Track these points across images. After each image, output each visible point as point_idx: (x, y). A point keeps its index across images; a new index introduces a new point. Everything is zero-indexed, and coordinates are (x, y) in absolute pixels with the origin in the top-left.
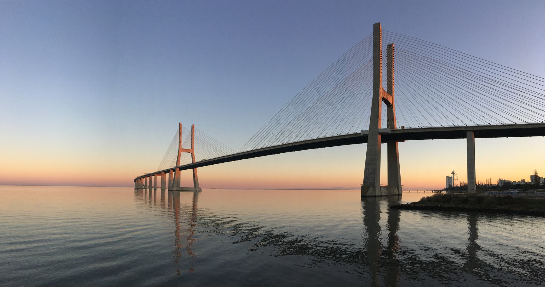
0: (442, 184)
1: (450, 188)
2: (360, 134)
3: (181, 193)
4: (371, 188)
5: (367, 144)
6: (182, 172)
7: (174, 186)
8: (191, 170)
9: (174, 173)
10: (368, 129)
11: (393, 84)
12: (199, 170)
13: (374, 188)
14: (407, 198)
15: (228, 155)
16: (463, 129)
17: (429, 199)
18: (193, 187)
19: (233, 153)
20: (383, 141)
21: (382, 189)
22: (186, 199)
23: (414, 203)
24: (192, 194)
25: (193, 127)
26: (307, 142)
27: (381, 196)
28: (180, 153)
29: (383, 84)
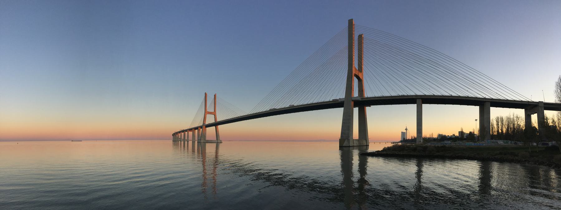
1: (404, 140)
5: (343, 108)
6: (207, 128)
7: (202, 139)
8: (214, 127)
9: (201, 129)
10: (344, 97)
11: (363, 64)
12: (220, 127)
13: (348, 140)
15: (241, 116)
16: (414, 97)
17: (389, 149)
18: (216, 139)
19: (245, 115)
20: (355, 107)
21: (355, 142)
22: (210, 149)
23: (378, 151)
24: (215, 145)
25: (215, 96)
27: (354, 146)
28: (206, 115)
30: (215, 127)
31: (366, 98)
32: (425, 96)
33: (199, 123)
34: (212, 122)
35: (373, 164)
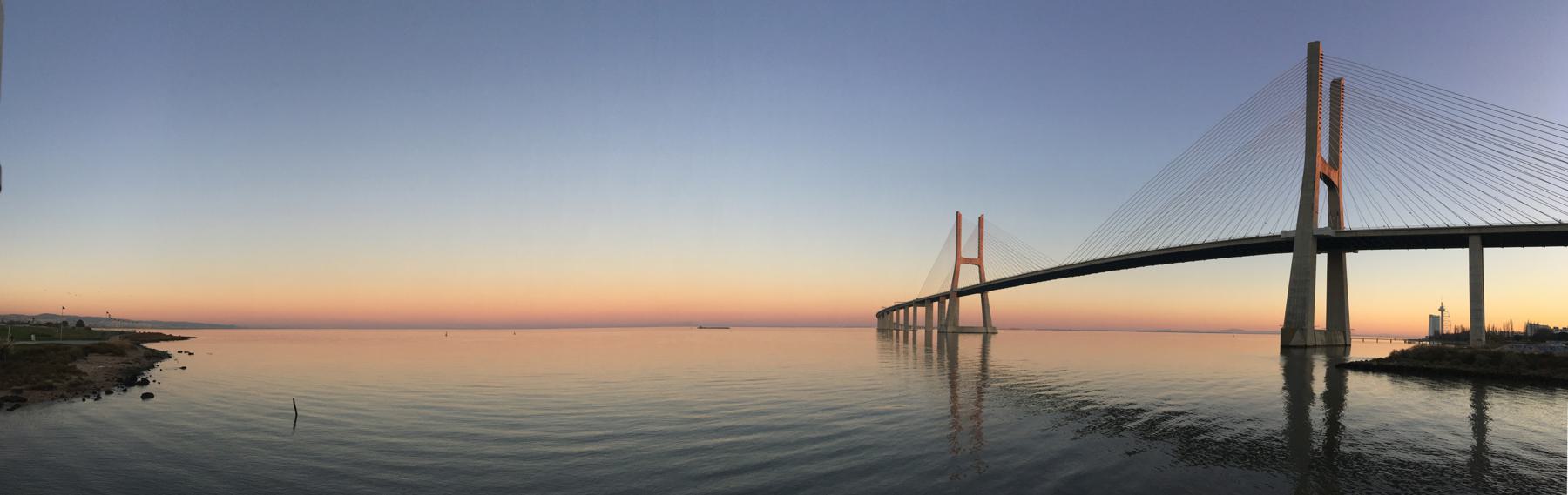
0: (1423, 329)
1: (1437, 334)
2: (1280, 236)
3: (961, 337)
4: (1298, 333)
5: (1292, 254)
6: (961, 298)
8: (978, 296)
9: (947, 301)
10: (1294, 227)
11: (1341, 149)
12: (991, 294)
13: (1303, 331)
14: (1360, 351)
16: (1462, 232)
17: (1404, 353)
18: (981, 325)
20: (1319, 252)
21: (1318, 334)
22: (969, 348)
23: (1379, 360)
24: (978, 339)
25: (981, 220)
26: (1186, 250)
27: (1315, 346)
28: (959, 267)
29: (1324, 151)
30: (980, 295)
31: (1347, 232)
32: (1491, 227)
33: (942, 286)
34: (973, 284)
35: (1356, 383)
